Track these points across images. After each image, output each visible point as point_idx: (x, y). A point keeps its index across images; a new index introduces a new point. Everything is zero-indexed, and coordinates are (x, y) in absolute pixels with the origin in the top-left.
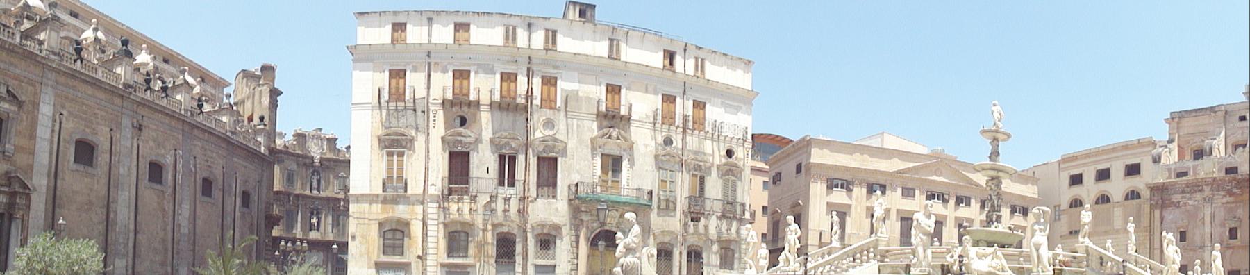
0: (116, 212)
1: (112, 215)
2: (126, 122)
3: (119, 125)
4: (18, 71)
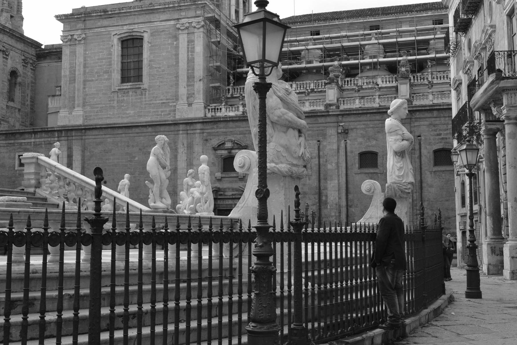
0: (326, 196)
1: (324, 198)
2: (332, 132)
3: (324, 135)
4: (241, 129)
